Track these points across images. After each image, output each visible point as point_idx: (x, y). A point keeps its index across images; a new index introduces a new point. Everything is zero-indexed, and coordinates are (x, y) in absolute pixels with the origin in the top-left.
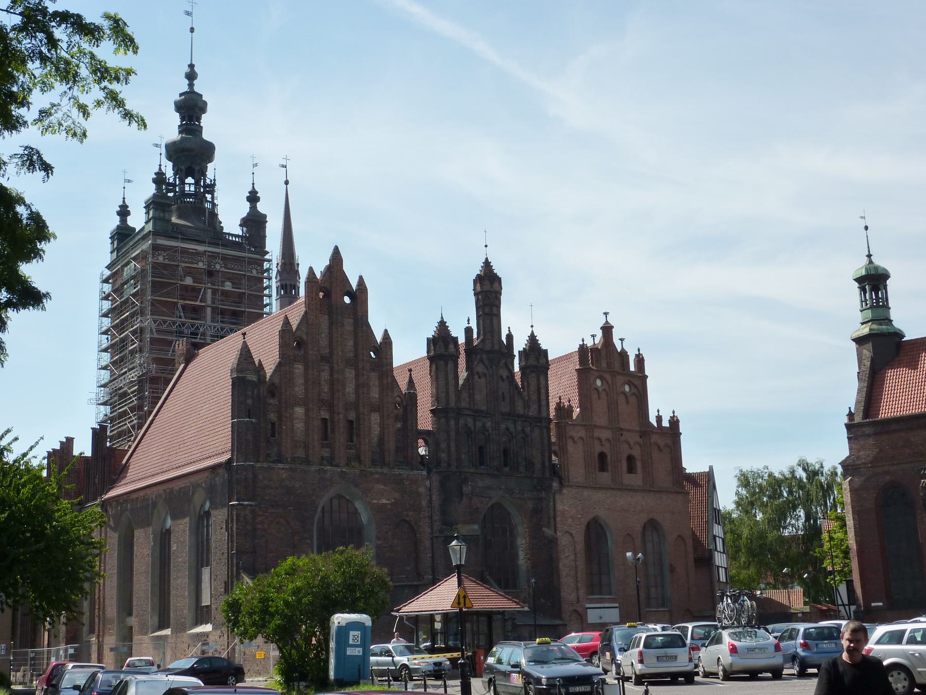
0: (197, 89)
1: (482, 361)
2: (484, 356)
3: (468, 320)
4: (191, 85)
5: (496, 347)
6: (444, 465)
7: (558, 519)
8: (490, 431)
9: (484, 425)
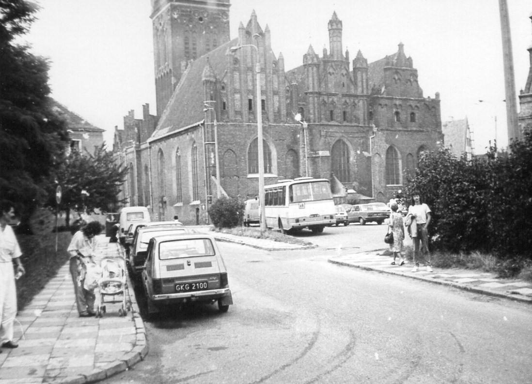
1: (332, 66)
2: (333, 64)
5: (340, 59)
6: (312, 121)
8: (336, 103)
9: (333, 101)
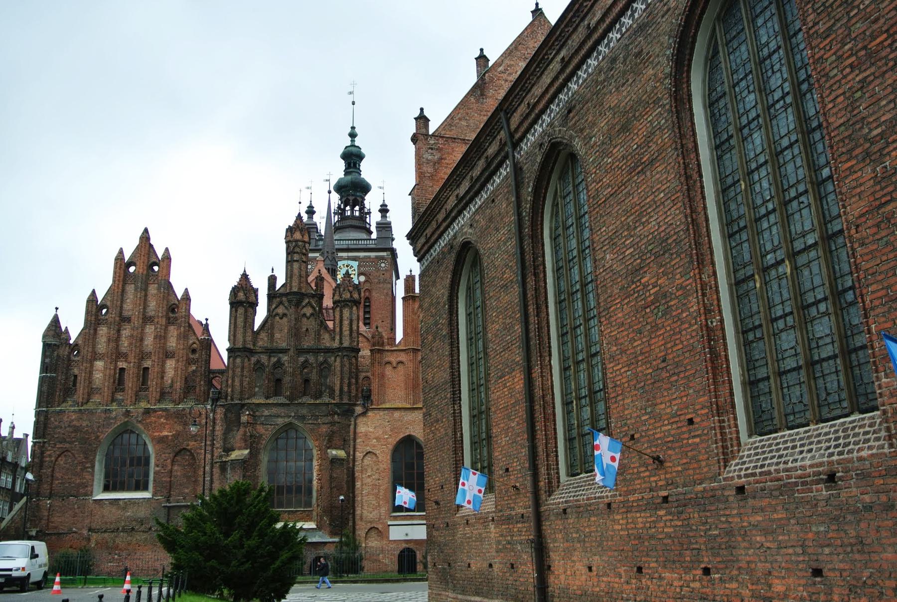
0: (356, 144)
3: (273, 270)
4: (353, 141)
7: (358, 441)
9: (279, 361)
